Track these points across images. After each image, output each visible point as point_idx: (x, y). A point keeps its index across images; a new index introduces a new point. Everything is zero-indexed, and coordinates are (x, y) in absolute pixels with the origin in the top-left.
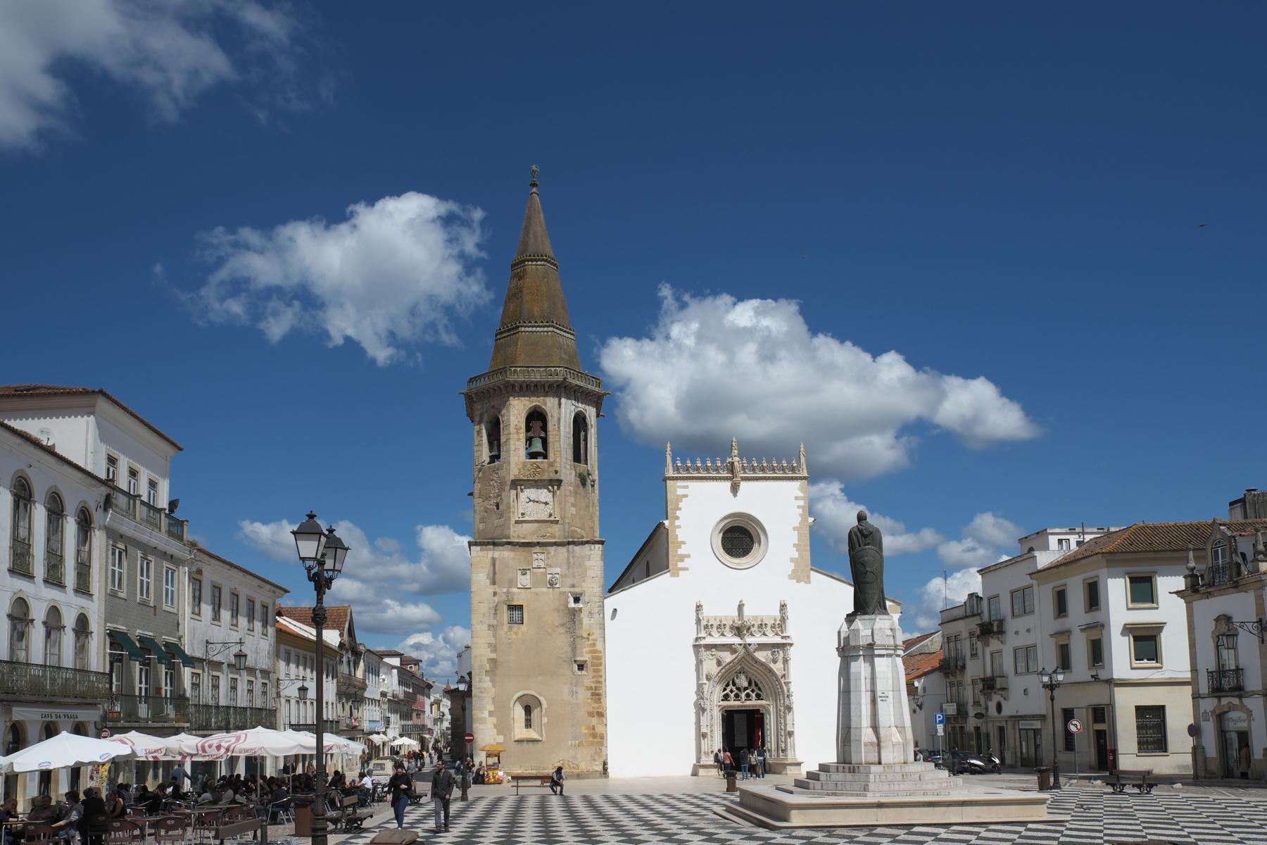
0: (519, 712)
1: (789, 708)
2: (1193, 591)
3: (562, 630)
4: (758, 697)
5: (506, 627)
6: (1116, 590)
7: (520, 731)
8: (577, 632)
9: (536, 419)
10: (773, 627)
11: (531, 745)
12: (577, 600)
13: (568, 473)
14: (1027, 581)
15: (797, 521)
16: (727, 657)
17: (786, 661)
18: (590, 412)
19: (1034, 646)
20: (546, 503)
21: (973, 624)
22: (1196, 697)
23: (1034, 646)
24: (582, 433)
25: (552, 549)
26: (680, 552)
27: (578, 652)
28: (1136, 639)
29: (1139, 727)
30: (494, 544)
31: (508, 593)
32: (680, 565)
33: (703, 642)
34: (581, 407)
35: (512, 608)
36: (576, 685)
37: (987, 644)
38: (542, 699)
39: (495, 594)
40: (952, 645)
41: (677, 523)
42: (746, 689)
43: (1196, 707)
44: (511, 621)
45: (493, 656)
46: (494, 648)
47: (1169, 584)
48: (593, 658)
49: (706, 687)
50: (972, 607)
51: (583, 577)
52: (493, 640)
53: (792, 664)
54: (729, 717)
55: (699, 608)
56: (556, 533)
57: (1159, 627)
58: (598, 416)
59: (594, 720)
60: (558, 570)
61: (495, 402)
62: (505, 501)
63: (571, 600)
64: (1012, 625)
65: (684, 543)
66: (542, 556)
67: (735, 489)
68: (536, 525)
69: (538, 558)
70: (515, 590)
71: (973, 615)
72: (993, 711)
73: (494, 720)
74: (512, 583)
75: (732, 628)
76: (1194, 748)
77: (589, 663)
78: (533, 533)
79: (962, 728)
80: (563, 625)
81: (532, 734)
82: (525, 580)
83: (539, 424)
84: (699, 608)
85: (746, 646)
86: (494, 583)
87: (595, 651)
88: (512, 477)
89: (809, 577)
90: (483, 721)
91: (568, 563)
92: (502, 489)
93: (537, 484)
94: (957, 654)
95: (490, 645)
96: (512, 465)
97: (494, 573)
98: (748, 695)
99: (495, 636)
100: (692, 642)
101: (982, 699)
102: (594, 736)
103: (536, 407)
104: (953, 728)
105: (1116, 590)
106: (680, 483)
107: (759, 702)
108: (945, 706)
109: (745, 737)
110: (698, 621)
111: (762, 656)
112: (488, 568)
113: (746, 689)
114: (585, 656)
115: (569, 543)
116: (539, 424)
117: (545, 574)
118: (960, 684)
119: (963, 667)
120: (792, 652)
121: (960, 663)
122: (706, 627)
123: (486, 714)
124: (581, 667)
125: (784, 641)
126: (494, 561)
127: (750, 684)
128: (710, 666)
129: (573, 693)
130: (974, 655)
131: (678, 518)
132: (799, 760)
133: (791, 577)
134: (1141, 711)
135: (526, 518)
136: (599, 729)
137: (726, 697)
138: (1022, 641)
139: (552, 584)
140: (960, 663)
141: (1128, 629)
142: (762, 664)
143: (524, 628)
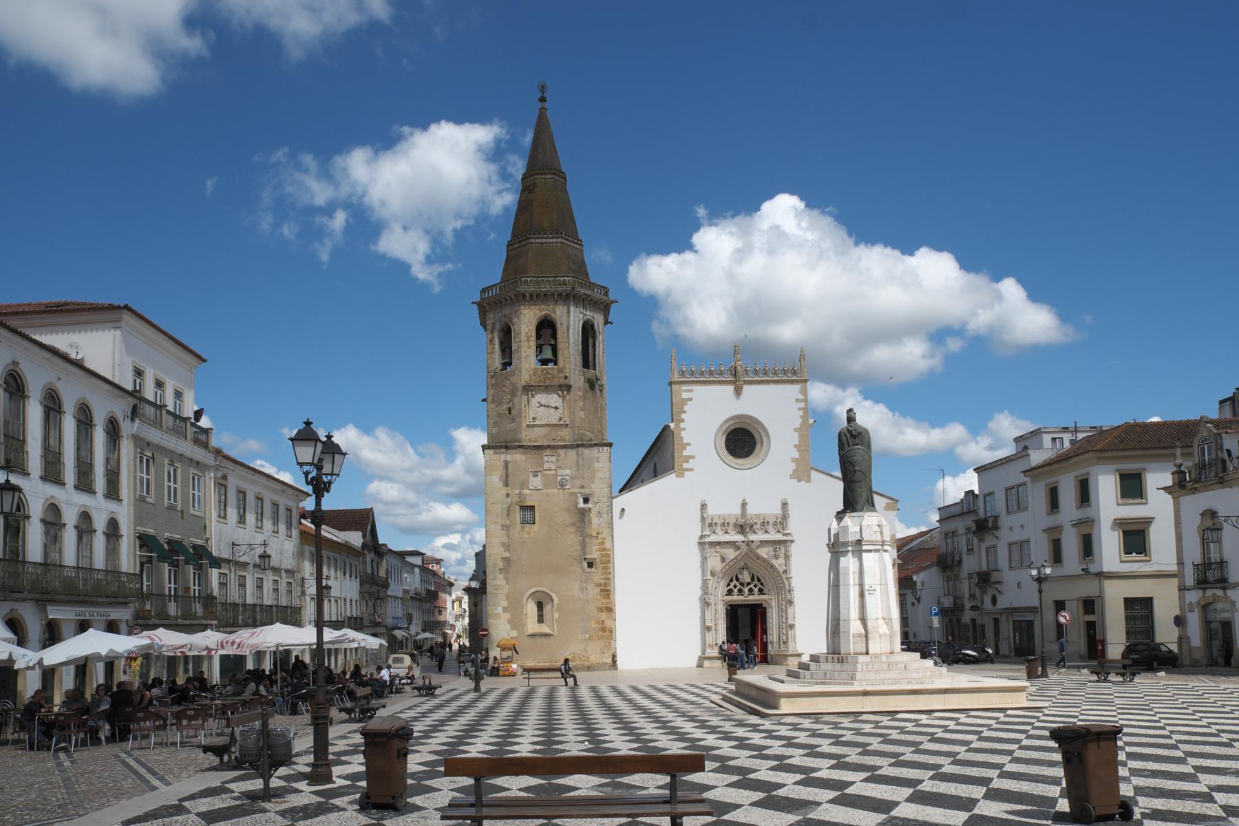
0: (532, 608)
1: (791, 602)
2: (1180, 487)
3: (572, 529)
4: (761, 591)
5: (518, 527)
6: (1106, 485)
7: (532, 626)
9: (546, 328)
10: (775, 524)
11: (543, 639)
12: (586, 500)
13: (577, 378)
14: (1022, 478)
15: (798, 423)
16: (731, 554)
17: (787, 557)
18: (598, 319)
19: (1028, 541)
20: (556, 408)
21: (969, 521)
22: (1182, 589)
23: (1028, 541)
24: (591, 340)
25: (562, 452)
26: (685, 453)
27: (588, 550)
28: (1125, 533)
29: (1127, 618)
30: (507, 447)
31: (520, 494)
32: (685, 466)
33: (707, 540)
34: (589, 314)
35: (524, 508)
36: (586, 581)
37: (981, 540)
38: (553, 595)
39: (508, 495)
40: (949, 541)
41: (682, 425)
42: (749, 584)
43: (1182, 599)
44: (524, 522)
45: (507, 554)
46: (507, 547)
47: (1158, 479)
49: (710, 583)
50: (968, 504)
51: (592, 479)
52: (506, 540)
53: (794, 560)
54: (733, 612)
55: (703, 506)
56: (566, 434)
57: (1148, 521)
58: (606, 322)
59: (604, 615)
60: (568, 472)
61: (507, 311)
62: (517, 407)
63: (581, 500)
64: (1006, 521)
65: (689, 444)
66: (553, 459)
67: (738, 392)
68: (545, 430)
69: (549, 460)
70: (526, 491)
71: (970, 512)
72: (988, 604)
73: (508, 615)
74: (524, 484)
75: (735, 525)
76: (1180, 638)
77: (598, 561)
78: (544, 437)
79: (959, 620)
80: (572, 525)
81: (545, 629)
82: (536, 482)
83: (549, 331)
84: (703, 506)
85: (749, 543)
86: (506, 485)
87: (604, 549)
88: (523, 383)
89: (809, 476)
90: (497, 616)
91: (578, 465)
92: (513, 394)
93: (547, 389)
94: (954, 548)
95: (503, 544)
96: (524, 372)
97: (507, 475)
98: (751, 590)
99: (508, 536)
100: (697, 540)
101: (978, 593)
102: (604, 630)
103: (546, 316)
104: (951, 620)
105: (1106, 485)
106: (684, 387)
107: (762, 597)
108: (942, 599)
109: (747, 630)
110: (703, 519)
111: (764, 552)
112: (501, 471)
113: (749, 584)
114: (594, 554)
115: (578, 446)
116: (549, 331)
117: (556, 476)
118: (957, 577)
119: (960, 562)
120: (793, 548)
121: (957, 558)
122: (710, 525)
123: (500, 610)
124: (590, 565)
125: (785, 538)
126: (506, 463)
127: (753, 579)
128: (715, 563)
129: (583, 590)
130: (970, 551)
131: (683, 421)
132: (800, 652)
133: (792, 477)
134: (1129, 602)
135: (537, 422)
136: (608, 624)
137: (730, 592)
138: (1017, 536)
139: (562, 485)
140: (957, 558)
141: (1119, 523)
142: (764, 560)
143: (535, 527)
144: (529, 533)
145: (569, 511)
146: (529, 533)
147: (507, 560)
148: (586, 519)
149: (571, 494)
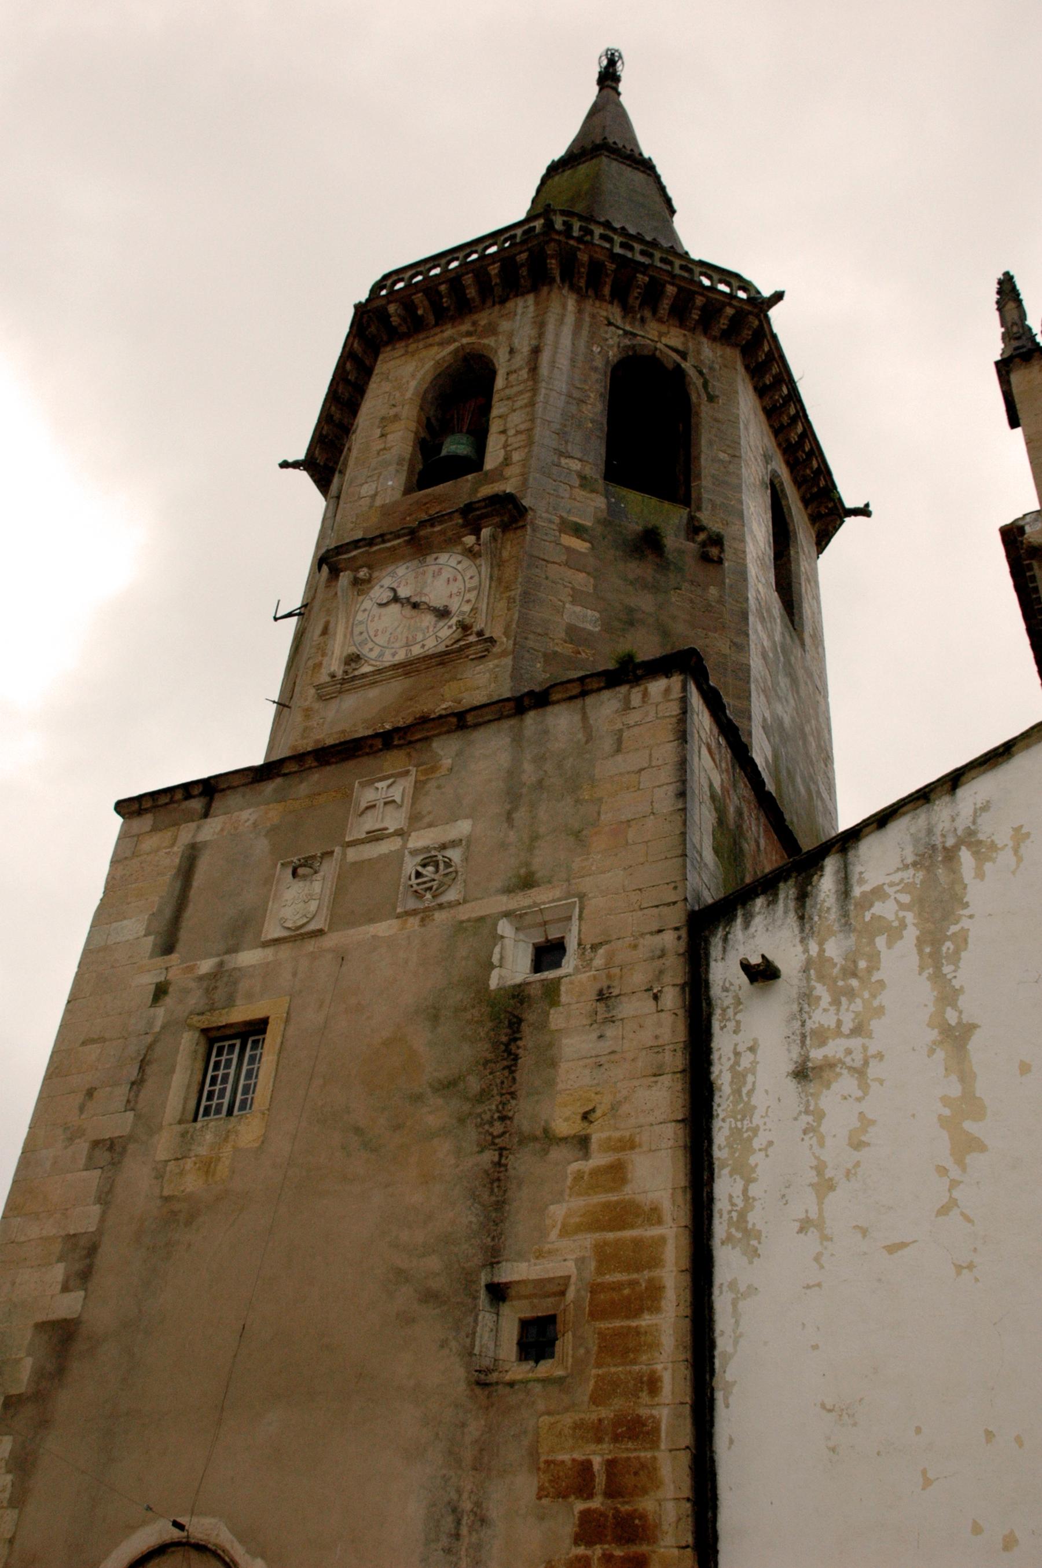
3: (436, 1114)
8: (526, 1114)
12: (549, 954)
34: (665, 338)
39: (160, 991)
45: (68, 1305)
46: (84, 1259)
48: (605, 1257)
74: (241, 930)
87: (623, 1215)
124: (538, 1339)
126: (192, 856)
144: (207, 1167)
145: (434, 1016)
146: (207, 1167)
147: (63, 1336)
148: (529, 1040)
149: (460, 927)
